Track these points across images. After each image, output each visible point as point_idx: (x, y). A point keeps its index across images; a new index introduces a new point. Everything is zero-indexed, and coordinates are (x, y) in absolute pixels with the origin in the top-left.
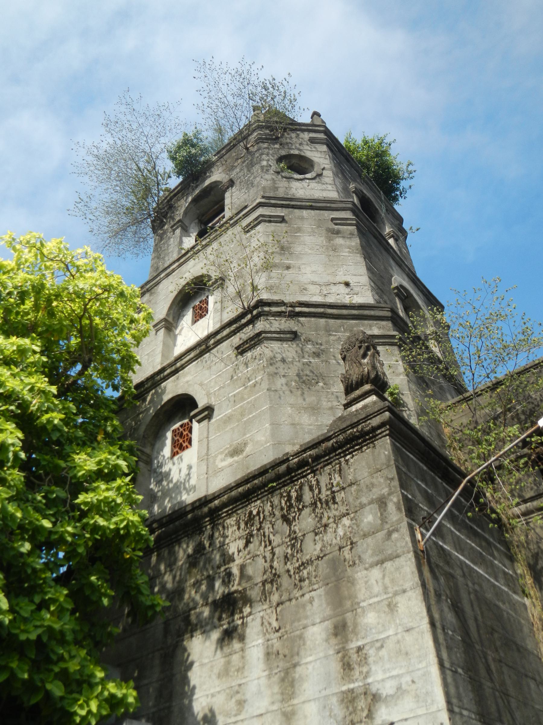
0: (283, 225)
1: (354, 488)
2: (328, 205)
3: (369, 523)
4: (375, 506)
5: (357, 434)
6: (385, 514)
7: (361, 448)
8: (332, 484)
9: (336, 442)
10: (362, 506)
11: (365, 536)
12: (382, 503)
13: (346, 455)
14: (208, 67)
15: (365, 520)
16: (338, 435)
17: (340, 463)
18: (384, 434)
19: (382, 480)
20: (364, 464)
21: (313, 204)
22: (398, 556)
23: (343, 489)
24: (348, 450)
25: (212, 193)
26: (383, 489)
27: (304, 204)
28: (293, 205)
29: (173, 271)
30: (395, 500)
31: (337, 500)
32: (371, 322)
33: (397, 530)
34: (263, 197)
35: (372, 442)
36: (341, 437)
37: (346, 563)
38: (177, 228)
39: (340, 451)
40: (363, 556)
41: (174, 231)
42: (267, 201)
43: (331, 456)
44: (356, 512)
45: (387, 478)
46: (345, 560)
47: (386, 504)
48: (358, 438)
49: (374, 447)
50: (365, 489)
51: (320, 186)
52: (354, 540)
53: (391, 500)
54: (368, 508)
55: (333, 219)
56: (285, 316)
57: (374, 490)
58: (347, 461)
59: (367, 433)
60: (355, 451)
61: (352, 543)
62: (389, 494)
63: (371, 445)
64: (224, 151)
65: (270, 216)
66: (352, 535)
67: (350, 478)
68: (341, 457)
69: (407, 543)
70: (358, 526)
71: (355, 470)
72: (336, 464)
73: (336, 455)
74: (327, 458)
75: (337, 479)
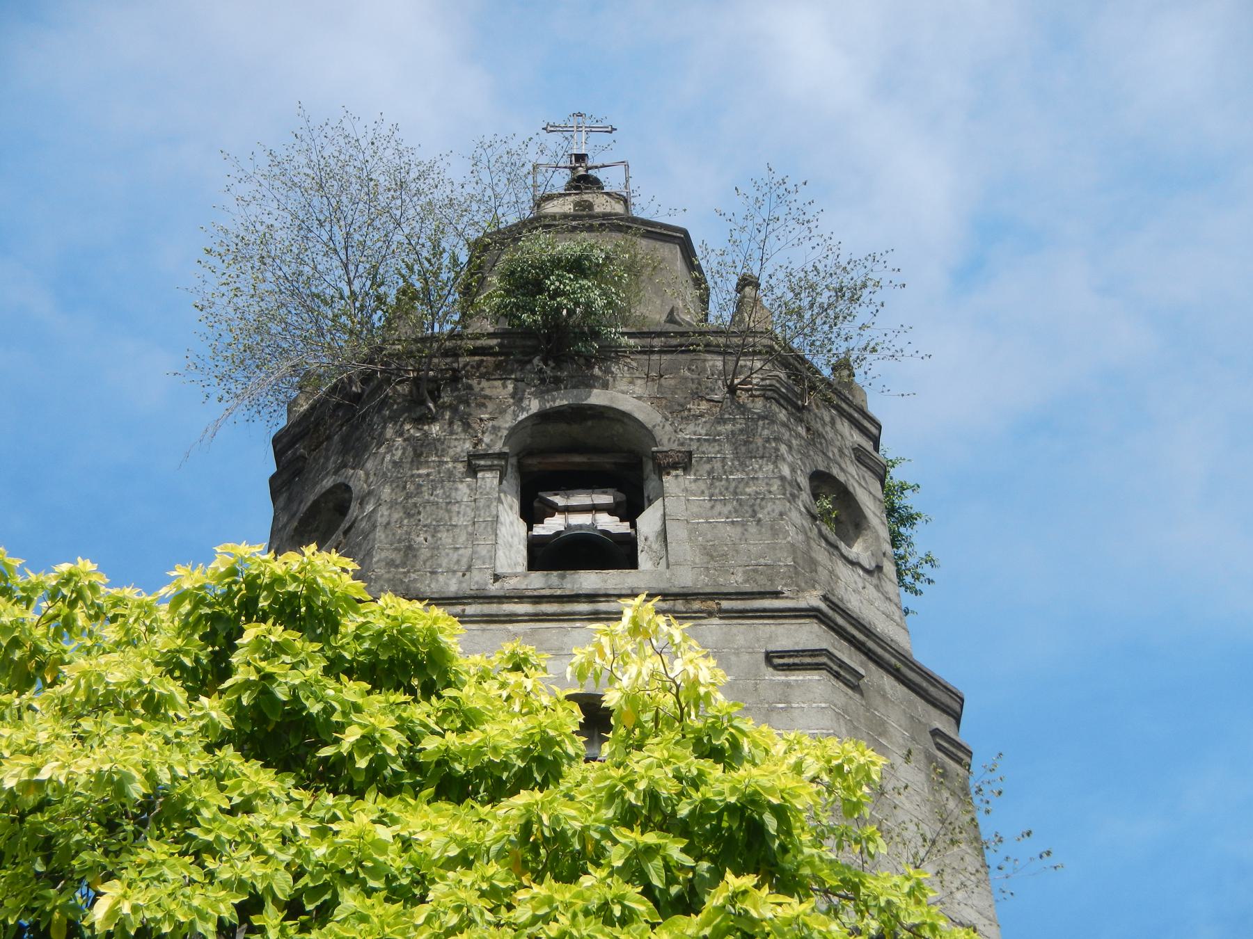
0: (857, 696)
2: (925, 684)
14: (781, 191)
21: (904, 670)
25: (590, 423)
27: (887, 656)
28: (870, 650)
29: (512, 618)
34: (825, 598)
38: (490, 468)
41: (472, 470)
42: (831, 613)
51: (871, 591)
55: (936, 733)
64: (657, 342)
65: (842, 664)
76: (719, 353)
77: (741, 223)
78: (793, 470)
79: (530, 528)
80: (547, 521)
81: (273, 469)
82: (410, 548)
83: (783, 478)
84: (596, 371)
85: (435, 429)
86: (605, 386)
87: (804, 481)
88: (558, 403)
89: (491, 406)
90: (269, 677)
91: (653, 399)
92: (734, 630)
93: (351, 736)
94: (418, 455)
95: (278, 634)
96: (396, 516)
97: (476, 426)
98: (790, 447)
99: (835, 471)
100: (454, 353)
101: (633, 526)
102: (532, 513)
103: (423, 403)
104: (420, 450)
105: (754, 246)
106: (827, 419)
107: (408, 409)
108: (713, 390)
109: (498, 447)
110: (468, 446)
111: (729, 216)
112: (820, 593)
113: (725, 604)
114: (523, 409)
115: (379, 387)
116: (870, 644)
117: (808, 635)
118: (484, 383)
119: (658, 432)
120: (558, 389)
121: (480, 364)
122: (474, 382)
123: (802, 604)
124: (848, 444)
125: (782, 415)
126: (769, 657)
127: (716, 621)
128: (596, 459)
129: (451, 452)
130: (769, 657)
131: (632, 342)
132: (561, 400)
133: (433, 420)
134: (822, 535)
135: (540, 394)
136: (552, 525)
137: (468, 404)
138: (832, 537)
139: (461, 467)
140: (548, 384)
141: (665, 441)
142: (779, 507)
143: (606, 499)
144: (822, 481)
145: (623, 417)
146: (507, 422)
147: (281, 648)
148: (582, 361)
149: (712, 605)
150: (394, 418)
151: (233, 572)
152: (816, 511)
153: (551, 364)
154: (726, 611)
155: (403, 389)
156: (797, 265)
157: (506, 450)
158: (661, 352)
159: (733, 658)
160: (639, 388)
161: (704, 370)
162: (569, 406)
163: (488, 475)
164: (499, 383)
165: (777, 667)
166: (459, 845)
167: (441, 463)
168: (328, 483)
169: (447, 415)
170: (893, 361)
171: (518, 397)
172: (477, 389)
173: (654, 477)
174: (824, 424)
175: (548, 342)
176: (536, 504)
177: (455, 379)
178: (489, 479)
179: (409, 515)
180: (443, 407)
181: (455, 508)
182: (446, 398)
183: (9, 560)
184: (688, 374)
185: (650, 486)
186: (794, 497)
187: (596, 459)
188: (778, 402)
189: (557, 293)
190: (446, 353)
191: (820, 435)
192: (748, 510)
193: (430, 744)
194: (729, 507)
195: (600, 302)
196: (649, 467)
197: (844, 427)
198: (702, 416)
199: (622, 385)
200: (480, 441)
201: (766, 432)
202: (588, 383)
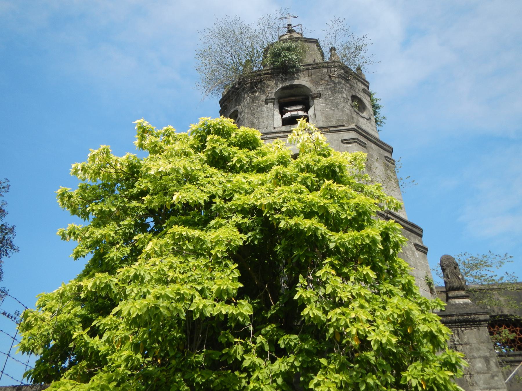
0: (365, 149)
1: (468, 346)
2: (383, 145)
3: (480, 367)
4: (483, 360)
5: (471, 320)
6: (489, 366)
7: (471, 327)
8: (454, 339)
9: (458, 319)
10: (475, 358)
11: (478, 373)
12: (487, 360)
13: (461, 327)
15: (477, 365)
16: (458, 316)
17: (458, 330)
18: (485, 325)
19: (485, 348)
20: (473, 336)
21: (377, 142)
22: (499, 388)
23: (462, 345)
24: (464, 325)
26: (486, 353)
27: (373, 139)
30: (494, 361)
31: (458, 349)
32: (415, 235)
33: (497, 376)
34: (356, 126)
35: (478, 327)
36: (461, 318)
37: (468, 383)
38: (271, 102)
39: (458, 324)
40: (478, 382)
41: (267, 103)
42: (357, 129)
43: (453, 325)
44: (471, 359)
45: (488, 348)
46: (467, 381)
47: (489, 362)
48: (470, 322)
49: (479, 329)
50: (475, 349)
51: (368, 124)
52: (472, 373)
53: (492, 360)
54: (478, 360)
55: (386, 157)
56: (383, 217)
57: (481, 351)
58: (462, 331)
59: (476, 321)
60: (467, 327)
61: (470, 374)
62: (491, 357)
63: (477, 328)
64: (310, 67)
65: (361, 141)
66: (470, 370)
67: (465, 340)
68: (459, 327)
69: (503, 383)
70: (473, 367)
71: (468, 337)
72: (455, 330)
73: (456, 325)
74: (450, 325)
75: (456, 338)
76: (326, 68)
77: (329, 32)
78: (347, 95)
79: (282, 116)
80: (286, 114)
81: (220, 108)
82: (253, 123)
83: (344, 97)
84: (295, 76)
85: (257, 94)
86: (298, 79)
87: (349, 98)
88: (286, 85)
89: (270, 87)
90: (215, 148)
91: (310, 81)
92: (333, 135)
93: (235, 159)
94: (253, 101)
95: (216, 137)
96: (249, 116)
97: (267, 92)
98: (346, 90)
99: (358, 95)
100: (260, 75)
101: (307, 113)
102: (282, 113)
103: (253, 88)
104: (254, 100)
105: (333, 38)
106: (355, 82)
107: (250, 90)
108: (325, 77)
109: (273, 97)
110: (265, 97)
111: (326, 31)
112: (354, 124)
113: (331, 129)
114: (278, 87)
115: (242, 85)
116: (368, 136)
117: (352, 135)
118: (268, 82)
119: (312, 89)
120: (286, 81)
121: (266, 77)
122: (265, 82)
123: (350, 127)
124: (361, 88)
125: (343, 82)
126: (342, 141)
127: (329, 133)
128: (297, 98)
129: (261, 99)
130: (342, 141)
131: (304, 67)
132: (287, 84)
133: (256, 92)
134: (355, 111)
135: (282, 83)
136: (288, 115)
137: (264, 87)
138: (357, 111)
139: (264, 103)
140: (284, 80)
141: (313, 91)
142: (343, 105)
143: (300, 107)
144: (354, 98)
145: (303, 86)
146: (274, 91)
147: (217, 141)
148: (292, 74)
149: (327, 130)
150: (247, 92)
151: (204, 124)
152: (353, 105)
153: (284, 75)
154: (331, 131)
155: (249, 85)
156: (344, 42)
157: (274, 97)
158: (311, 69)
159: (333, 142)
160: (307, 79)
161: (323, 73)
162: (289, 85)
163: (271, 104)
164: (271, 81)
165: (345, 143)
166: (261, 181)
167: (259, 102)
168: (232, 110)
169: (259, 90)
170: (371, 64)
171: (276, 84)
172: (266, 83)
173: (312, 101)
174: (354, 84)
175: (283, 69)
176: (283, 110)
177: (261, 81)
178: (271, 105)
179: (252, 115)
180: (258, 89)
181: (263, 113)
182: (259, 86)
183: (152, 127)
184: (319, 74)
185: (311, 103)
186: (347, 102)
187: (297, 98)
188: (342, 78)
189: (284, 56)
190: (258, 75)
191: (354, 86)
192: (336, 106)
193: (255, 160)
194: (330, 106)
195: (295, 58)
196: (310, 98)
197: (359, 84)
198: (323, 84)
199: (302, 79)
200: (268, 96)
201: (339, 87)
202: (294, 79)
